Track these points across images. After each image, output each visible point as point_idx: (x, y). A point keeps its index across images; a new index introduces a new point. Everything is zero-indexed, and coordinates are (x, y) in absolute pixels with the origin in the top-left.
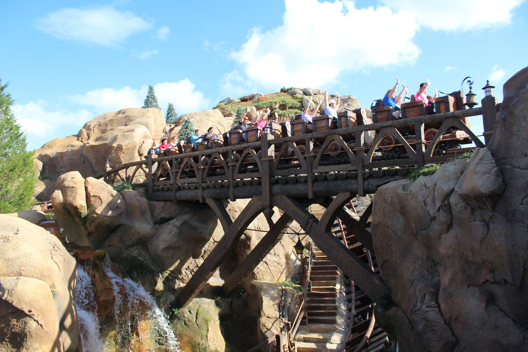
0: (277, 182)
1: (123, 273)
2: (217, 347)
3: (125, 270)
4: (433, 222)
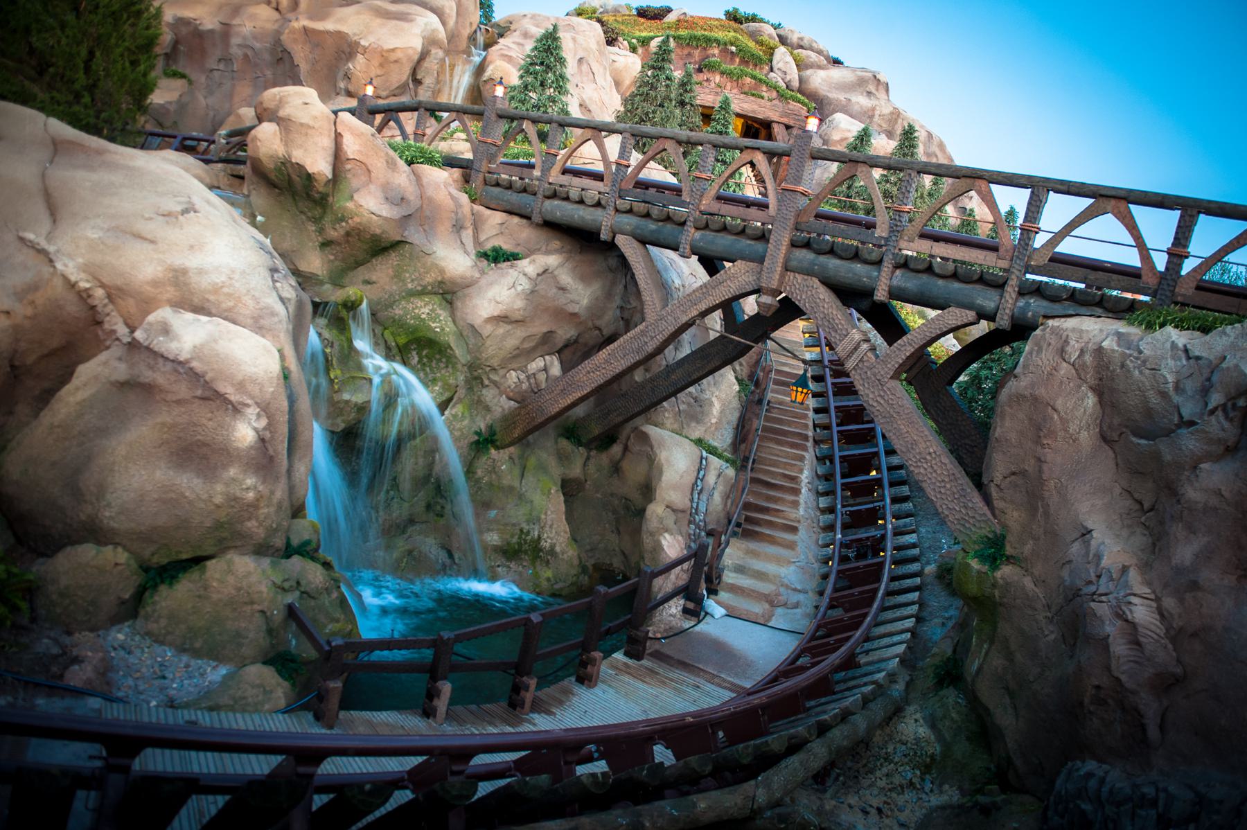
0: (807, 245)
1: (388, 348)
2: (555, 544)
3: (393, 344)
4: (1183, 431)
